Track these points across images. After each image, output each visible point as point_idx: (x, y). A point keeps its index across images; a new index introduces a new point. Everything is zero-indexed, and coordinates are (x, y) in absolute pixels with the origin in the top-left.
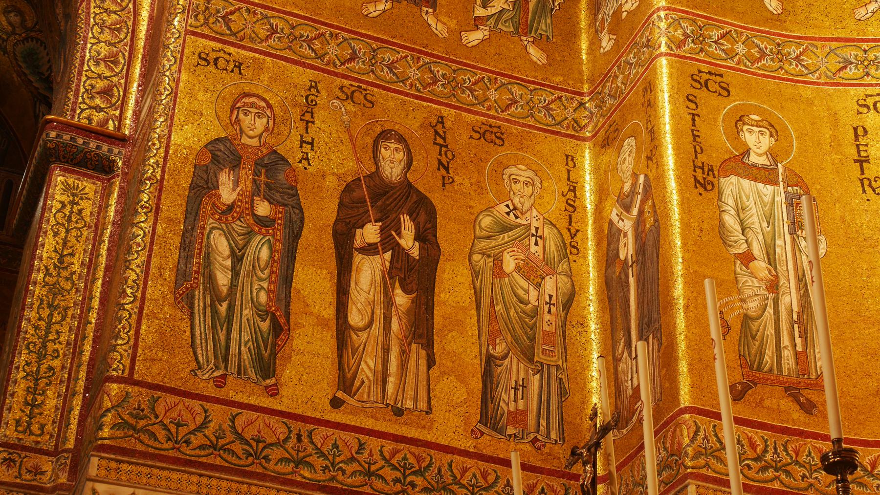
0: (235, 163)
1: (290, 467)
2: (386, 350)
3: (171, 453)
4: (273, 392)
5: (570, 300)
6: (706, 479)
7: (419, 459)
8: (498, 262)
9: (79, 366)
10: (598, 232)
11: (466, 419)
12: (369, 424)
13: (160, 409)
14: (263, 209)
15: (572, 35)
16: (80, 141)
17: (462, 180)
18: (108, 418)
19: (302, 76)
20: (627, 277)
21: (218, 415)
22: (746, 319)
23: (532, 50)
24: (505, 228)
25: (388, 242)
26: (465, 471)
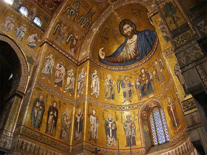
0: (39, 102)
1: (40, 140)
2: (51, 127)
3: (28, 136)
4: (39, 130)
5: (70, 125)
6: (86, 149)
7: (53, 141)
8: (64, 119)
9: (15, 122)
10: (74, 117)
11: (59, 137)
12: (49, 136)
13: (27, 130)
14: (41, 108)
15: (74, 94)
16: (19, 93)
17: (61, 108)
18: (21, 130)
19: (47, 92)
20: (78, 124)
21: (33, 132)
22: (91, 132)
23: (70, 95)
24: (65, 115)
25: (53, 114)
26: (58, 143)
